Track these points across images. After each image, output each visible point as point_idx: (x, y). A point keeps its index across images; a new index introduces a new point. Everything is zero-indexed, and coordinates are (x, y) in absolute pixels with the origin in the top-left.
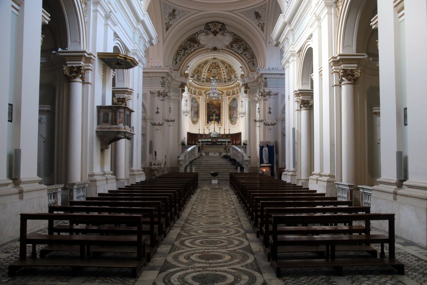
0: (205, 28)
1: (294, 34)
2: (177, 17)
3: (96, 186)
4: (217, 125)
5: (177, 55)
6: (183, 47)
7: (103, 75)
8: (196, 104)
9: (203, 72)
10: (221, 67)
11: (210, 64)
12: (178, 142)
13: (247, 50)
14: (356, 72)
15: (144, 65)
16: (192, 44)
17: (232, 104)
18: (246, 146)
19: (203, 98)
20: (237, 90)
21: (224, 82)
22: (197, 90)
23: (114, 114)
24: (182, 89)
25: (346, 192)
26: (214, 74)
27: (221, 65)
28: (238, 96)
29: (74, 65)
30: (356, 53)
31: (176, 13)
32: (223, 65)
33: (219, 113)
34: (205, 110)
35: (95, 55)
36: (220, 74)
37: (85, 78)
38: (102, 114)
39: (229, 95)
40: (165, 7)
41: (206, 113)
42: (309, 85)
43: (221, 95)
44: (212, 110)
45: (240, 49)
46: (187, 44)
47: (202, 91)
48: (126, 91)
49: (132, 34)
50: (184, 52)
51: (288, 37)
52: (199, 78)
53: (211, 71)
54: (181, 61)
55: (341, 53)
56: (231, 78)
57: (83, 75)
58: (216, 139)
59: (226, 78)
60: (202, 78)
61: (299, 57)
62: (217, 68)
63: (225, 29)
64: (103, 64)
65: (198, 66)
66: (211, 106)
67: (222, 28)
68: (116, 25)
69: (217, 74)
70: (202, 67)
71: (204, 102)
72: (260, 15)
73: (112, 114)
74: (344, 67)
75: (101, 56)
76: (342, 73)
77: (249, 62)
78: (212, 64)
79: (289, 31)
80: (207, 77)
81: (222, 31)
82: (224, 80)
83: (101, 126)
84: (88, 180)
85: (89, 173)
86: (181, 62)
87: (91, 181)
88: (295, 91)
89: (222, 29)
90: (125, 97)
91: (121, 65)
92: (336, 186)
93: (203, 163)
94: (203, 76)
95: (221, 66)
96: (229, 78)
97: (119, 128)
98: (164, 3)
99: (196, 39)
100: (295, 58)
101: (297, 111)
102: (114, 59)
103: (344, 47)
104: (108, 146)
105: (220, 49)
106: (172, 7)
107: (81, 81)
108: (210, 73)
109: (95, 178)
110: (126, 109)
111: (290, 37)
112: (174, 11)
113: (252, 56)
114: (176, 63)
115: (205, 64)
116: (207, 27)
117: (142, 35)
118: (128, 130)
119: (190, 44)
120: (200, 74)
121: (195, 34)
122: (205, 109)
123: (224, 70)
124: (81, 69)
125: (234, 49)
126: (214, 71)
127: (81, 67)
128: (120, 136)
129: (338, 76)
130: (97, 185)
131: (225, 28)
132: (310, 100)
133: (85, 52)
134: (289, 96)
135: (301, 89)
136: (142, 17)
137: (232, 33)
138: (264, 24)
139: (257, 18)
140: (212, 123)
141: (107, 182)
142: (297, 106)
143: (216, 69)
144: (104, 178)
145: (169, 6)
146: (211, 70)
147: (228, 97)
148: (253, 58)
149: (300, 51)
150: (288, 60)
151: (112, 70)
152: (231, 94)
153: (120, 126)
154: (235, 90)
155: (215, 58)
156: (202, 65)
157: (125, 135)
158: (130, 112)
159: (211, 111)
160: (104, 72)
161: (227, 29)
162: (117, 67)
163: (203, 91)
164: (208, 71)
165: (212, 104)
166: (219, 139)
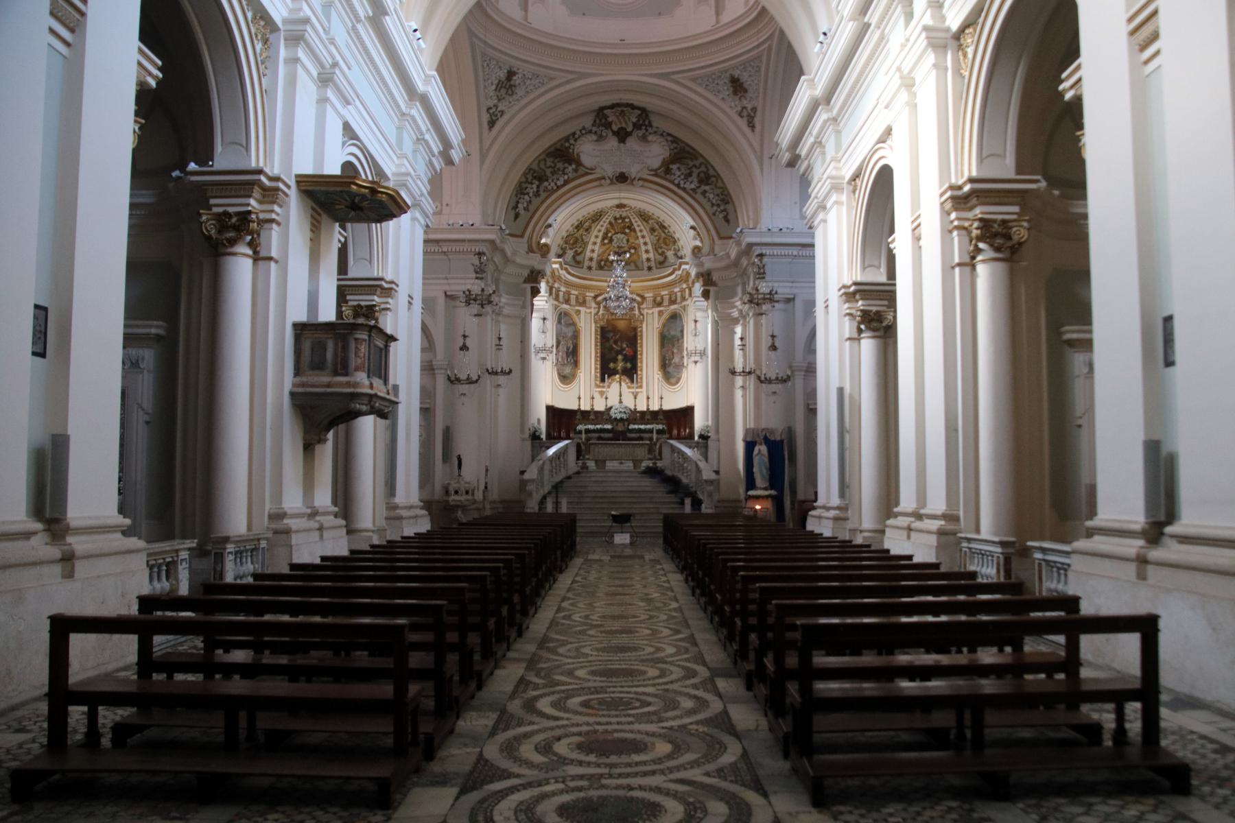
0: (595, 121)
1: (838, 132)
2: (520, 92)
3: (291, 546)
4: (629, 387)
5: (519, 196)
6: (535, 172)
7: (311, 240)
8: (572, 328)
9: (590, 243)
10: (637, 229)
11: (608, 221)
12: (522, 431)
13: (710, 182)
14: (1017, 226)
15: (428, 217)
16: (560, 165)
17: (668, 330)
18: (707, 443)
19: (591, 313)
20: (683, 291)
21: (646, 269)
22: (573, 292)
23: (340, 345)
24: (532, 287)
25: (992, 561)
28: (684, 308)
29: (231, 210)
30: (1018, 173)
31: (517, 80)
33: (632, 353)
34: (596, 345)
35: (290, 180)
36: (637, 247)
37: (260, 244)
38: (307, 346)
39: (660, 304)
40: (485, 65)
41: (596, 353)
42: (882, 270)
43: (640, 304)
45: (690, 179)
46: (545, 164)
47: (588, 294)
48: (377, 286)
49: (395, 130)
50: (538, 187)
51: (823, 141)
52: (578, 258)
53: (611, 240)
54: (528, 210)
55: (974, 174)
56: (666, 258)
57: (255, 236)
58: (626, 423)
59: (653, 259)
60: (587, 258)
61: (854, 192)
62: (627, 231)
63: (651, 126)
64: (313, 209)
67: (641, 122)
68: (348, 103)
69: (626, 249)
70: (587, 230)
71: (593, 325)
72: (745, 85)
73: (336, 345)
74: (982, 213)
75: (306, 186)
76: (977, 229)
77: (714, 214)
78: (613, 221)
79: (825, 122)
80: (598, 256)
81: (640, 129)
82: (646, 265)
83: (304, 379)
84: (268, 528)
85: (271, 509)
86: (529, 214)
87: (276, 532)
88: (844, 287)
89: (641, 125)
90: (374, 303)
91: (361, 209)
92: (965, 544)
93: (589, 489)
94: (588, 254)
95: (639, 226)
96: (661, 258)
97: (356, 385)
98: (483, 55)
99: (571, 151)
100: (844, 198)
101: (848, 343)
102: (341, 192)
103: (981, 159)
104: (325, 436)
105: (635, 178)
106: (504, 64)
107: (250, 252)
108: (607, 246)
109: (287, 524)
110: (374, 331)
111: (827, 141)
112: (511, 74)
113: (722, 197)
114: (517, 216)
115: (594, 222)
116: (601, 120)
117: (422, 134)
118: (379, 388)
119: (555, 166)
121: (567, 139)
122: (596, 342)
124: (249, 218)
125: (673, 177)
126: (618, 239)
127: (250, 212)
128: (358, 406)
129: (967, 239)
130: (293, 542)
131: (650, 122)
132: (884, 312)
133: (260, 172)
134: (826, 302)
135: (859, 279)
136: (423, 85)
137: (669, 135)
138: (754, 109)
139: (735, 93)
140: (613, 380)
141: (321, 537)
142: (848, 327)
143: (625, 233)
144: (313, 524)
145: (498, 62)
146: (611, 237)
147: (657, 310)
148: (727, 203)
149: (856, 176)
150: (823, 200)
151: (337, 224)
152: (666, 303)
153: (358, 380)
154: (677, 290)
156: (587, 224)
157: (372, 403)
158: (386, 342)
159: (611, 346)
160: (314, 229)
161: (654, 124)
162: (350, 216)
163: (591, 294)
164: (604, 239)
165: (615, 330)
166: (634, 424)
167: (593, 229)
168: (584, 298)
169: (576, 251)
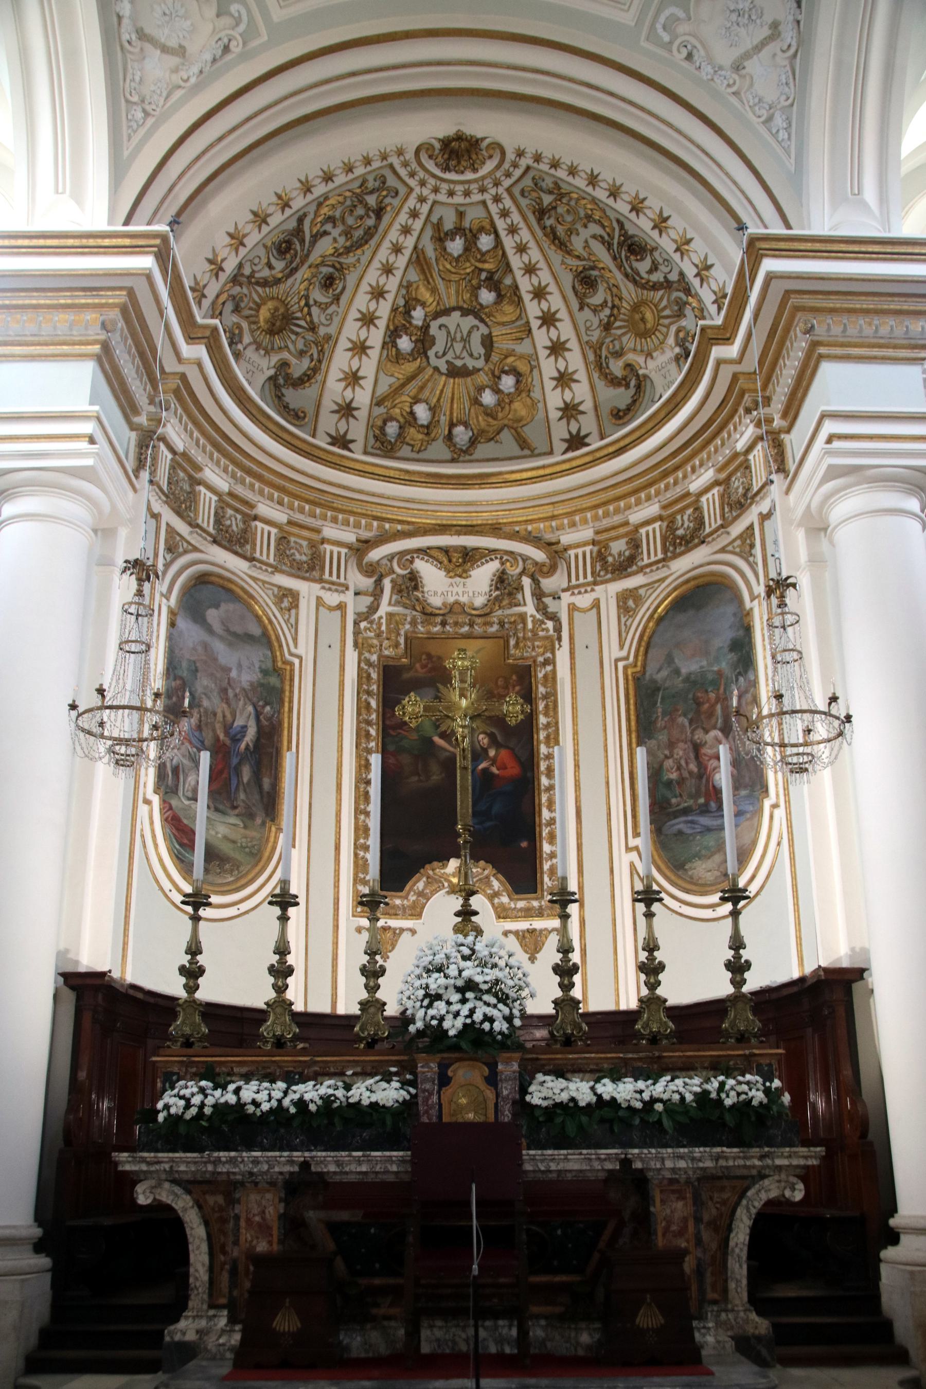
4: (502, 913)
8: (256, 656)
9: (343, 344)
10: (525, 285)
11: (409, 242)
17: (670, 659)
19: (341, 607)
22: (264, 509)
26: (455, 372)
27: (534, 254)
33: (513, 770)
36: (522, 367)
39: (623, 568)
43: (537, 572)
47: (330, 531)
53: (424, 342)
58: (509, 1068)
59: (587, 406)
60: (328, 404)
62: (487, 297)
65: (284, 248)
70: (328, 282)
71: (352, 657)
80: (378, 402)
82: (560, 431)
96: (621, 397)
108: (410, 367)
120: (306, 363)
123: (563, 314)
140: (435, 884)
143: (474, 311)
146: (426, 328)
152: (652, 551)
156: (325, 247)
159: (430, 741)
164: (393, 334)
166: (560, 1073)
167: (351, 279)
168: (313, 545)
169: (284, 364)
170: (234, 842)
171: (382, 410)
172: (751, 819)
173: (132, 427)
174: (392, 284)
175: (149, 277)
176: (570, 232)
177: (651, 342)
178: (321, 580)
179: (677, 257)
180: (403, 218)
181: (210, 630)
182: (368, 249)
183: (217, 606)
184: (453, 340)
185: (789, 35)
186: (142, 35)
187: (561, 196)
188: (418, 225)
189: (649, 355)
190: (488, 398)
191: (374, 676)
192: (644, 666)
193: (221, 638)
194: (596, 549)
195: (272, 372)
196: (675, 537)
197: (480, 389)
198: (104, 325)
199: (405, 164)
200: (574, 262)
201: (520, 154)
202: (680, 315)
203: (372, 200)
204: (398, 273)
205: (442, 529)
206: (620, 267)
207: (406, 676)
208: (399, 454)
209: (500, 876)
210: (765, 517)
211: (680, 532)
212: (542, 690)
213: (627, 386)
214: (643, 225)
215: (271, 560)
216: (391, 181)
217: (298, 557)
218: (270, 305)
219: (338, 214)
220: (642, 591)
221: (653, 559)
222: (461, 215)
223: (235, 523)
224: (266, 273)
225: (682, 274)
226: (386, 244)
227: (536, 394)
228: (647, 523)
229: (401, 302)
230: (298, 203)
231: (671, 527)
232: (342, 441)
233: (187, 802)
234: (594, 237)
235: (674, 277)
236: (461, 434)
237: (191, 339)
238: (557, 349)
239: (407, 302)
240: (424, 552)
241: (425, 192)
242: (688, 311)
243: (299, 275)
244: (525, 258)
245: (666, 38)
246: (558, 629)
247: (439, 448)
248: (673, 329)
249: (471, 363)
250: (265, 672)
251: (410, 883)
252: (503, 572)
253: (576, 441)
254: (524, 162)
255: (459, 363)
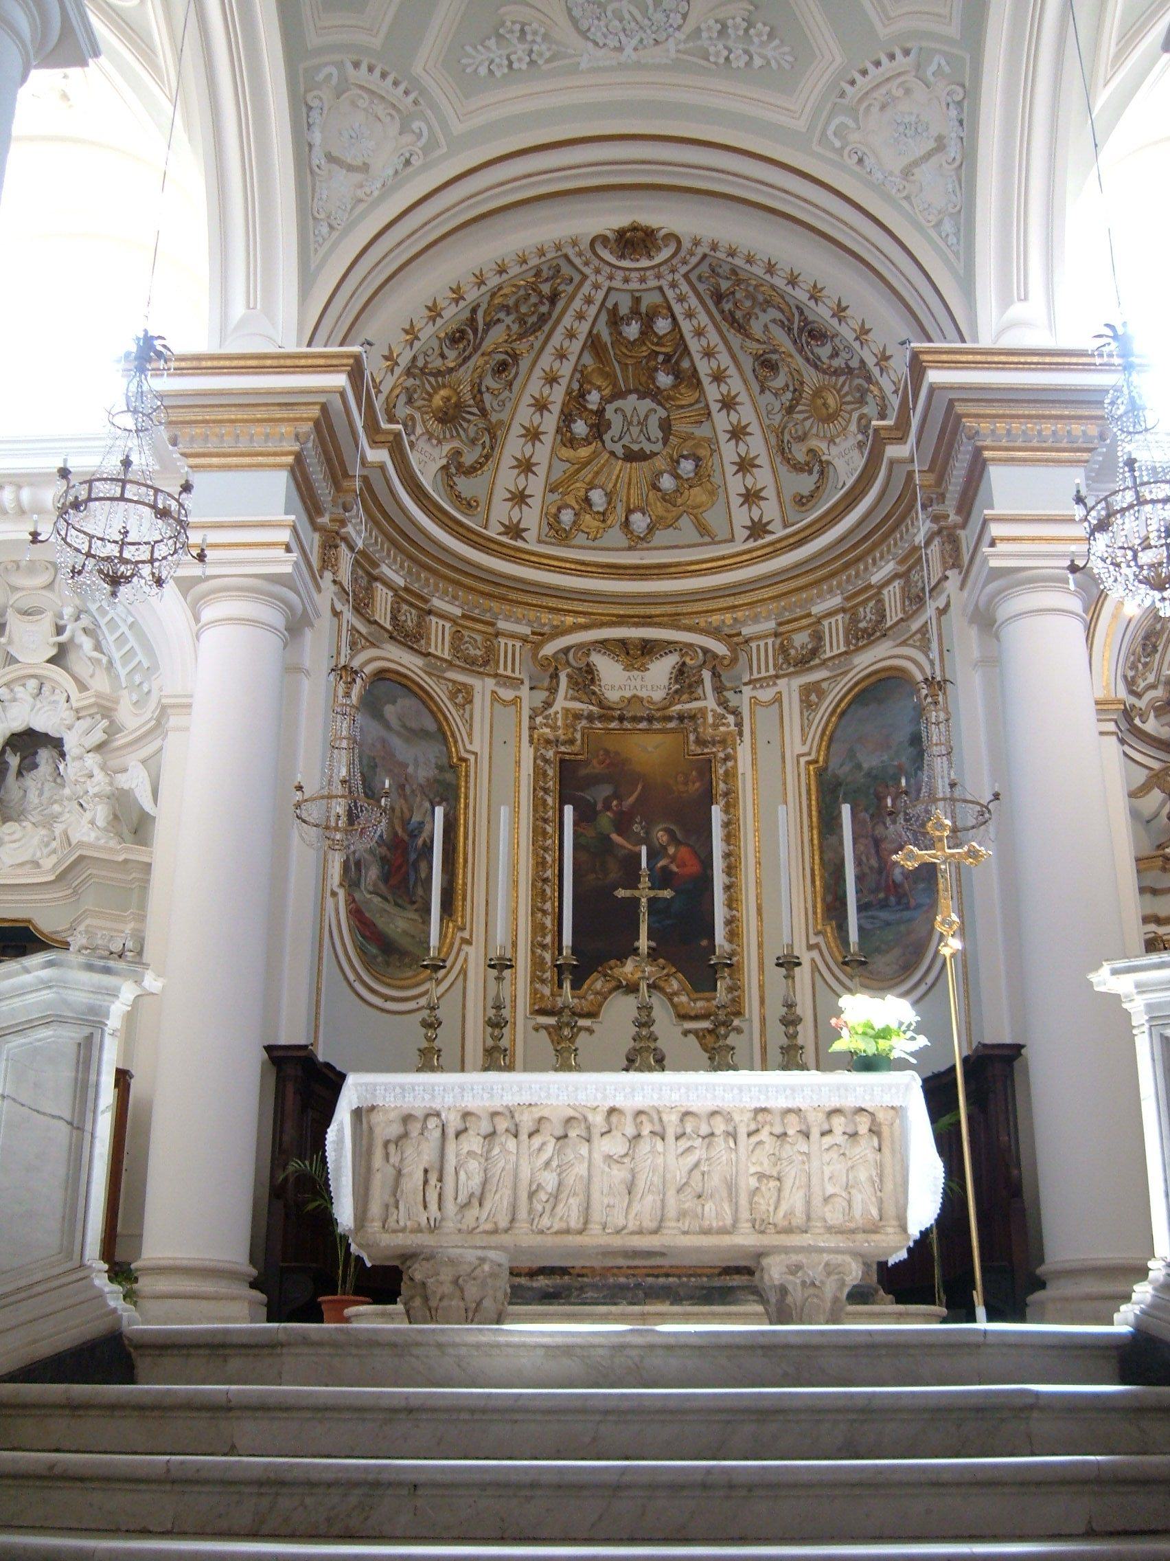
9: (516, 430)
11: (583, 329)
17: (851, 754)
19: (516, 701)
27: (713, 337)
32: (732, 336)
39: (804, 662)
44: (615, 837)
53: (599, 427)
62: (664, 380)
65: (456, 338)
66: (605, 791)
70: (502, 368)
71: (527, 753)
82: (742, 517)
108: (584, 452)
123: (743, 398)
143: (653, 393)
146: (600, 412)
147: (790, 688)
152: (834, 645)
155: (635, 228)
156: (497, 335)
164: (567, 418)
167: (524, 364)
169: (458, 453)
170: (413, 937)
171: (556, 496)
172: (927, 911)
173: (316, 527)
174: (566, 369)
175: (342, 394)
176: (748, 316)
177: (832, 428)
178: (496, 675)
179: (856, 345)
180: (577, 304)
181: (387, 726)
182: (541, 336)
183: (394, 702)
184: (630, 423)
185: (953, 150)
186: (330, 158)
187: (739, 282)
188: (593, 310)
189: (832, 441)
190: (667, 482)
191: (550, 772)
192: (826, 761)
193: (398, 734)
194: (778, 641)
195: (444, 462)
196: (858, 629)
197: (659, 474)
198: (297, 437)
199: (580, 254)
200: (754, 347)
201: (697, 243)
202: (862, 401)
203: (546, 289)
204: (573, 358)
205: (621, 621)
206: (801, 350)
207: (583, 772)
208: (574, 542)
209: (680, 975)
210: (943, 612)
211: (862, 625)
212: (722, 786)
213: (810, 472)
214: (822, 313)
215: (446, 656)
216: (566, 270)
217: (472, 652)
218: (443, 393)
219: (511, 302)
220: (825, 685)
221: (836, 652)
222: (637, 300)
223: (409, 617)
224: (437, 363)
225: (862, 361)
226: (560, 330)
227: (717, 479)
228: (830, 614)
229: (576, 386)
230: (472, 295)
231: (854, 620)
232: (515, 531)
233: (369, 896)
234: (774, 321)
235: (854, 364)
236: (639, 522)
237: (374, 443)
238: (737, 433)
239: (581, 386)
240: (603, 646)
241: (600, 279)
242: (869, 398)
243: (471, 364)
244: (704, 342)
245: (838, 144)
246: (739, 724)
247: (615, 536)
248: (855, 415)
249: (648, 448)
250: (441, 768)
251: (588, 982)
252: (684, 664)
253: (758, 529)
254: (700, 251)
255: (635, 447)
